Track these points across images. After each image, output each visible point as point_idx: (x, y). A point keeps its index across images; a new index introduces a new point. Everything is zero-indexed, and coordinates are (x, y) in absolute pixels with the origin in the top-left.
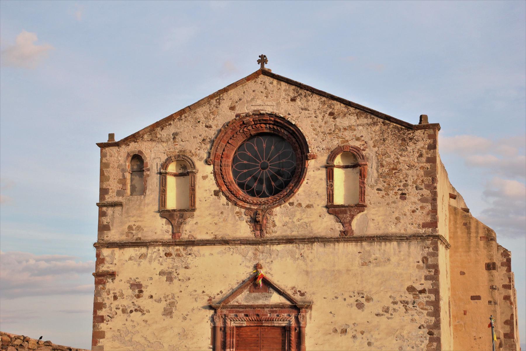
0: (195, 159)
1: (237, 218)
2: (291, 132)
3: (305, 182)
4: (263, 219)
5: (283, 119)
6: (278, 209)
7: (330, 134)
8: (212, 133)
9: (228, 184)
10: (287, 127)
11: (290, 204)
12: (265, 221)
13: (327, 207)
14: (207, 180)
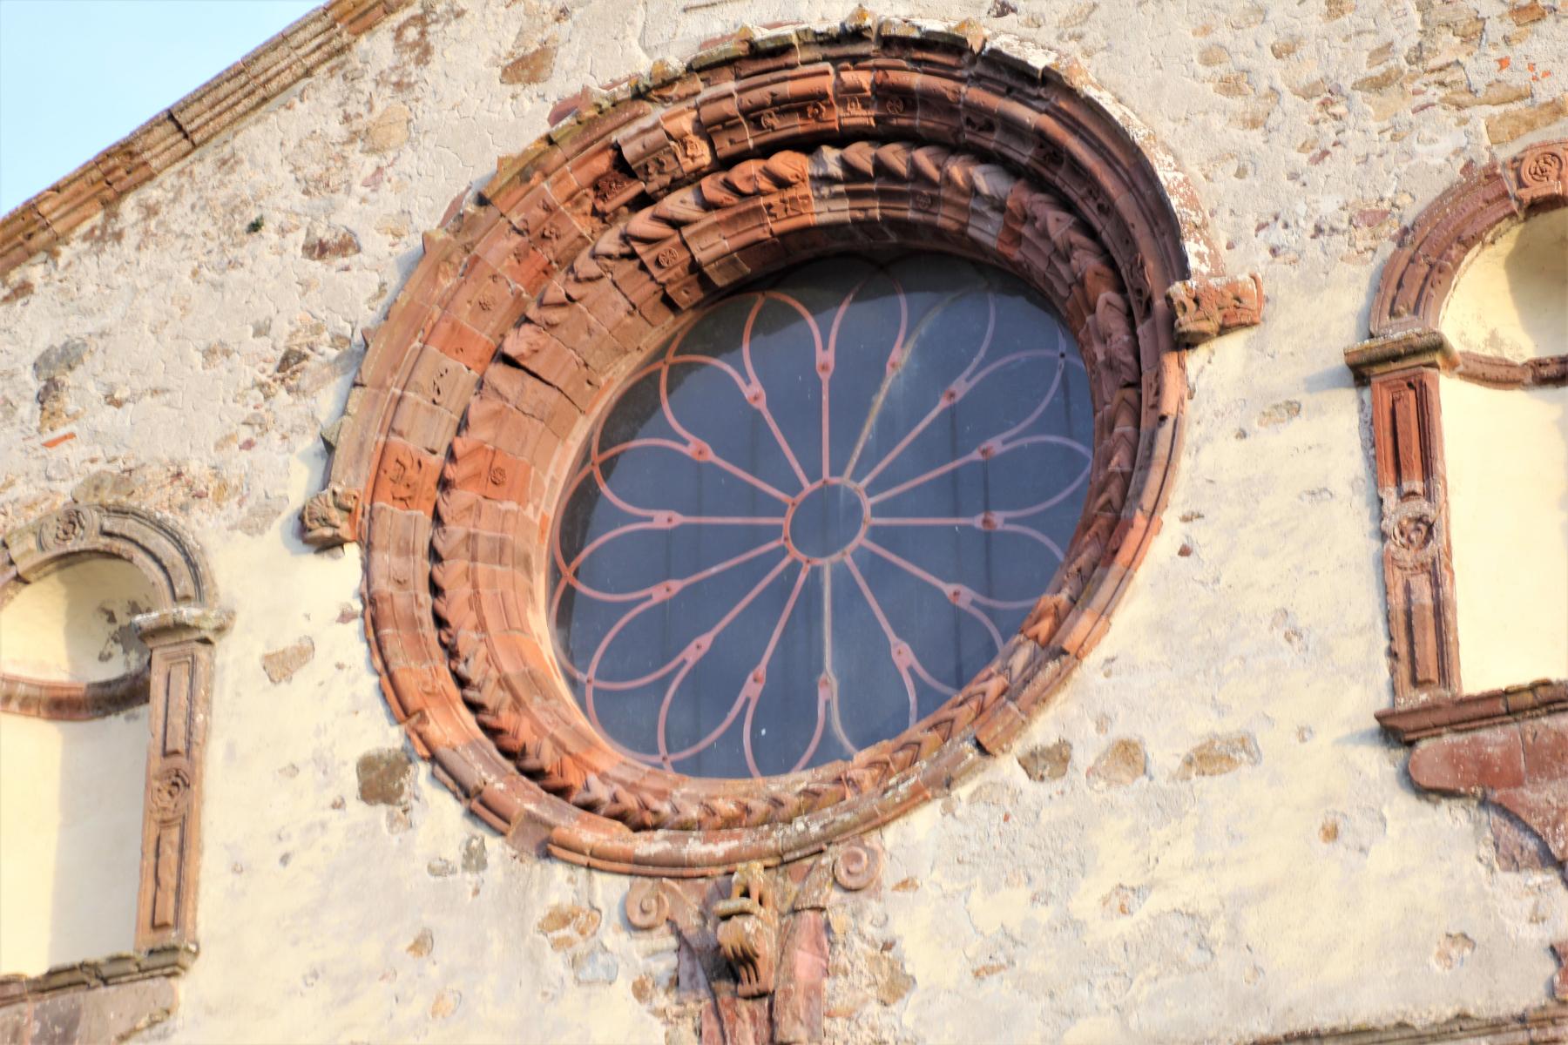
0: (206, 528)
1: (556, 964)
2: (1025, 155)
3: (1161, 548)
4: (786, 939)
5: (946, 47)
6: (925, 822)
7: (1378, 85)
8: (357, 294)
9: (490, 695)
10: (989, 121)
11: (1032, 763)
12: (804, 961)
13: (1394, 731)
14: (304, 681)
